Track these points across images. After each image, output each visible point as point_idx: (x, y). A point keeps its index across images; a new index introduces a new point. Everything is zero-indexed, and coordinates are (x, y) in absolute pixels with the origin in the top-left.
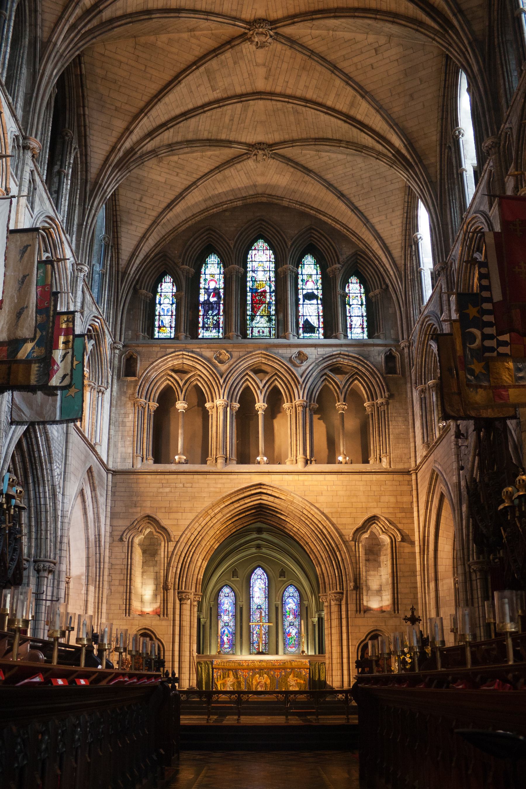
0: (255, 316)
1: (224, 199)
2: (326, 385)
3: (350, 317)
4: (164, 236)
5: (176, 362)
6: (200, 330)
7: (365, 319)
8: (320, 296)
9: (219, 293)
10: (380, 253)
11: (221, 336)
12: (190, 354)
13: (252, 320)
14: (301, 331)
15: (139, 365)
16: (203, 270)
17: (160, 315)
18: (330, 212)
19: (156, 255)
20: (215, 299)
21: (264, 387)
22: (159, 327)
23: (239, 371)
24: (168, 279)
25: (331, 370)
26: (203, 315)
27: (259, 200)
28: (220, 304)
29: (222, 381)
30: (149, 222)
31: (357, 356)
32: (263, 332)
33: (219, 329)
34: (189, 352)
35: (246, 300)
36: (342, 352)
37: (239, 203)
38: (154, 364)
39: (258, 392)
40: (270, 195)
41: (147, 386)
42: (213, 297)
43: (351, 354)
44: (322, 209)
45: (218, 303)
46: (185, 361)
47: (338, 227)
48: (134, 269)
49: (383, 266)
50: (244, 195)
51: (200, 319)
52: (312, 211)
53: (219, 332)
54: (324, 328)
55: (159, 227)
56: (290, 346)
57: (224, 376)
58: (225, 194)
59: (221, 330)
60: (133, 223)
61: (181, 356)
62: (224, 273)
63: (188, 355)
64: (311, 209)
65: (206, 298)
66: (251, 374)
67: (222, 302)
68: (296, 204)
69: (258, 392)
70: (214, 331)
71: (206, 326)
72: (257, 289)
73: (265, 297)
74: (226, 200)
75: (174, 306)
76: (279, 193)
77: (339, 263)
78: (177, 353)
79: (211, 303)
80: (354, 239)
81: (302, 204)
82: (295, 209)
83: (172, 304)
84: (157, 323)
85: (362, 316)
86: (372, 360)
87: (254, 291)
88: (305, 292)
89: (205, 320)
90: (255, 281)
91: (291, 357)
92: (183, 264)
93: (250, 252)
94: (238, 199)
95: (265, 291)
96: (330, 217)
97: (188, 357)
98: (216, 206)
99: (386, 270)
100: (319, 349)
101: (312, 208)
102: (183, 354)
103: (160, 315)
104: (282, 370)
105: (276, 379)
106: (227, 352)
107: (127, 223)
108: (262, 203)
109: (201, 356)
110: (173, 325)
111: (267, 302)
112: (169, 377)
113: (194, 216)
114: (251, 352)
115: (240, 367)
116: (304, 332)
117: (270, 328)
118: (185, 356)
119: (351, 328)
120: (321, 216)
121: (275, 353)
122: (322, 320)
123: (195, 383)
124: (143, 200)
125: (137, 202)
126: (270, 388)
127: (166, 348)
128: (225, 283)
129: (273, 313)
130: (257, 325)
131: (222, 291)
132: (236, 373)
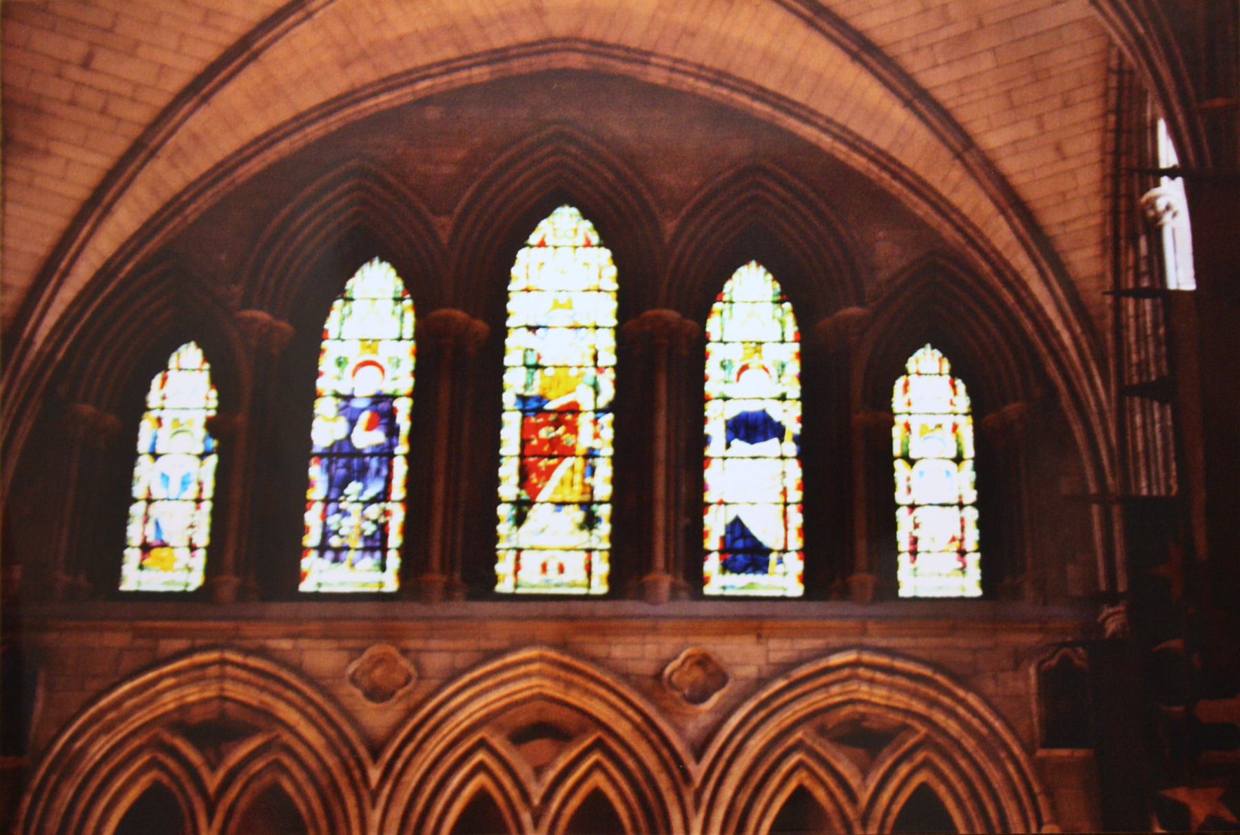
0: (531, 503)
1: (421, 59)
2: (801, 791)
3: (912, 507)
4: (178, 196)
5: (192, 694)
6: (310, 563)
7: (972, 514)
8: (793, 427)
9: (391, 414)
10: (1021, 261)
11: (391, 584)
12: (252, 662)
13: (520, 520)
14: (712, 565)
15: (39, 705)
16: (331, 324)
17: (150, 501)
18: (826, 107)
19: (141, 269)
20: (378, 437)
21: (547, 797)
22: (146, 548)
23: (449, 731)
24: (189, 357)
25: (822, 731)
26: (327, 501)
27: (558, 61)
28: (391, 456)
29: (375, 774)
30: (119, 145)
31: (927, 672)
32: (561, 569)
33: (384, 557)
34: (248, 652)
35: (497, 443)
36: (867, 657)
37: (480, 74)
38: (104, 702)
39: (526, 818)
40: (600, 44)
41: (68, 793)
42: (371, 427)
43: (899, 664)
44: (798, 97)
45: (385, 453)
46: (235, 691)
47: (858, 161)
48: (51, 319)
49: (1036, 313)
50: (498, 43)
51: (312, 518)
52: (757, 105)
53: (383, 568)
54: (805, 553)
55: (159, 166)
56: (653, 628)
57: (389, 754)
58: (425, 39)
59: (394, 561)
60: (57, 148)
61: (213, 670)
62: (418, 336)
63: (244, 667)
64: (754, 97)
65: (341, 434)
66: (498, 742)
67: (402, 448)
68: (698, 77)
69: (526, 818)
70: (369, 562)
71: (335, 541)
72: (541, 399)
73: (573, 429)
74: (428, 59)
75: (213, 460)
76: (633, 38)
77: (860, 303)
78: (199, 658)
79: (360, 454)
80: (922, 209)
81: (720, 77)
82: (693, 94)
83: (203, 456)
84: (135, 532)
85: (961, 506)
86: (990, 687)
87: (532, 406)
88: (732, 410)
89: (333, 521)
90: (537, 367)
91: (658, 676)
92: (247, 303)
93: (522, 254)
94: (473, 59)
95: (574, 409)
96: (829, 126)
97: (244, 674)
98: (389, 83)
99: (1045, 327)
100: (773, 644)
101: (760, 93)
102: (223, 662)
103: (150, 501)
104: (623, 728)
105: (597, 765)
106: (405, 652)
107: (29, 149)
108: (566, 74)
109: (298, 670)
110: (202, 539)
111: (581, 449)
112: (161, 757)
113: (301, 121)
114: (500, 653)
115: (452, 713)
116: (726, 567)
117: (589, 551)
118: (230, 670)
119: (914, 553)
120: (792, 123)
121: (593, 660)
122: (796, 519)
123: (268, 778)
124: (97, 63)
125: (75, 73)
126: (575, 803)
127: (156, 635)
128: (419, 373)
129: (603, 490)
130: (536, 542)
131: (403, 408)
132: (433, 741)
